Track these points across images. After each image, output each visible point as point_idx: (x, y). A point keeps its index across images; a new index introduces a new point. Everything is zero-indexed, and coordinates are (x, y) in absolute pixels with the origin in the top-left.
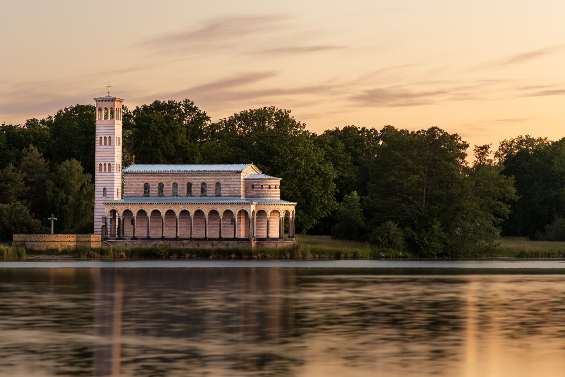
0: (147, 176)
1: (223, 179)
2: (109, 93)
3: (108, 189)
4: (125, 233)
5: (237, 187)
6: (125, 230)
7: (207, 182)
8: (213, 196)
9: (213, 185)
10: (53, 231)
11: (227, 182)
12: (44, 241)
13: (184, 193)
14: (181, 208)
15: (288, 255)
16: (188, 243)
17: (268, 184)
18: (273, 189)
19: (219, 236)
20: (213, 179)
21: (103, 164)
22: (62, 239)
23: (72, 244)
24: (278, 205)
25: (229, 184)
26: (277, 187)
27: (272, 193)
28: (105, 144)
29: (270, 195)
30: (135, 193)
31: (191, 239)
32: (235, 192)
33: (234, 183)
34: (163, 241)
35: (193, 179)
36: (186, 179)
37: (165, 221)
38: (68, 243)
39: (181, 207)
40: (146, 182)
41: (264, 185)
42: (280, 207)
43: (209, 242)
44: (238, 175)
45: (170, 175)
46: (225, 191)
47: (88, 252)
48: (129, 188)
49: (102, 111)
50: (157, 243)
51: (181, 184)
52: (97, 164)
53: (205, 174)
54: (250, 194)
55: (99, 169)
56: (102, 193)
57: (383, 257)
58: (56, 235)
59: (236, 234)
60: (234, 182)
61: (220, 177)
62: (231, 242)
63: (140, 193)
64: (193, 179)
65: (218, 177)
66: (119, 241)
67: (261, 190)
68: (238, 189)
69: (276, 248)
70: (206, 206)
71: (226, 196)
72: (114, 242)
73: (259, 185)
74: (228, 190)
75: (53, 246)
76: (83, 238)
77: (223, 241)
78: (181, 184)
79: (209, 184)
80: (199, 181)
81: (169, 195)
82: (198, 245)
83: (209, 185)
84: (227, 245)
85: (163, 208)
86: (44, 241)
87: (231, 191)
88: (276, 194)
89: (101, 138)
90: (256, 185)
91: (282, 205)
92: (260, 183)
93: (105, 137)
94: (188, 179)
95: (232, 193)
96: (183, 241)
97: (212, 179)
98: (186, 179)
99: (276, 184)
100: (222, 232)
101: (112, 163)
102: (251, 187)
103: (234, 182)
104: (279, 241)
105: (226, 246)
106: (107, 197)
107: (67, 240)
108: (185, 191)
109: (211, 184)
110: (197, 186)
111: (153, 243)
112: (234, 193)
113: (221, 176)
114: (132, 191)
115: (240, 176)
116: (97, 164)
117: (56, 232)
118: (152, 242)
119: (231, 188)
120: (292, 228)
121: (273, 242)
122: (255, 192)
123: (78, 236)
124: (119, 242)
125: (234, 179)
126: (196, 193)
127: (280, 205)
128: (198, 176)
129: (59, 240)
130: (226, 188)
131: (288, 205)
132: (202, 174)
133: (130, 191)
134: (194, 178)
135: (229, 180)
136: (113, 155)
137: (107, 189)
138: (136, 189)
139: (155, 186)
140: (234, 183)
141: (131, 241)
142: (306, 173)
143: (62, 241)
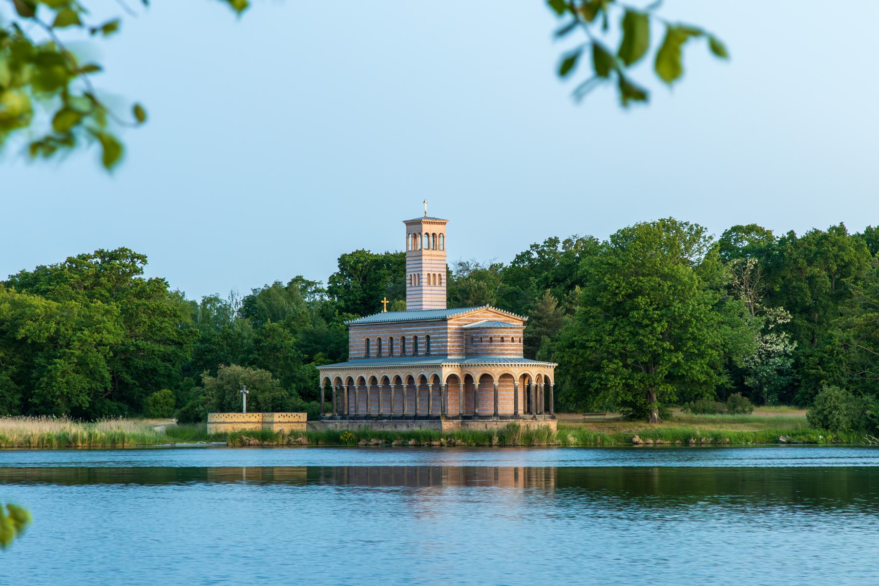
0: (368, 329)
8: (424, 355)
10: (244, 409)
12: (214, 423)
15: (496, 440)
22: (235, 419)
23: (249, 427)
26: (515, 339)
27: (495, 349)
28: (435, 283)
31: (389, 418)
35: (407, 331)
37: (370, 393)
38: (243, 424)
39: (382, 371)
40: (366, 337)
42: (493, 370)
47: (241, 439)
49: (418, 238)
54: (470, 351)
57: (783, 443)
58: (250, 414)
59: (430, 411)
62: (424, 422)
64: (407, 331)
69: (485, 430)
70: (404, 370)
71: (435, 355)
72: (327, 422)
73: (477, 337)
75: (222, 428)
76: (268, 417)
82: (396, 426)
83: (420, 339)
85: (367, 374)
86: (214, 423)
88: (515, 349)
89: (411, 275)
99: (513, 335)
100: (418, 407)
104: (490, 420)
107: (243, 421)
113: (430, 325)
115: (447, 324)
117: (248, 411)
119: (439, 342)
120: (539, 400)
121: (480, 420)
122: (474, 348)
123: (264, 415)
127: (447, 367)
128: (410, 327)
129: (230, 421)
136: (420, 300)
142: (646, 316)
143: (235, 422)
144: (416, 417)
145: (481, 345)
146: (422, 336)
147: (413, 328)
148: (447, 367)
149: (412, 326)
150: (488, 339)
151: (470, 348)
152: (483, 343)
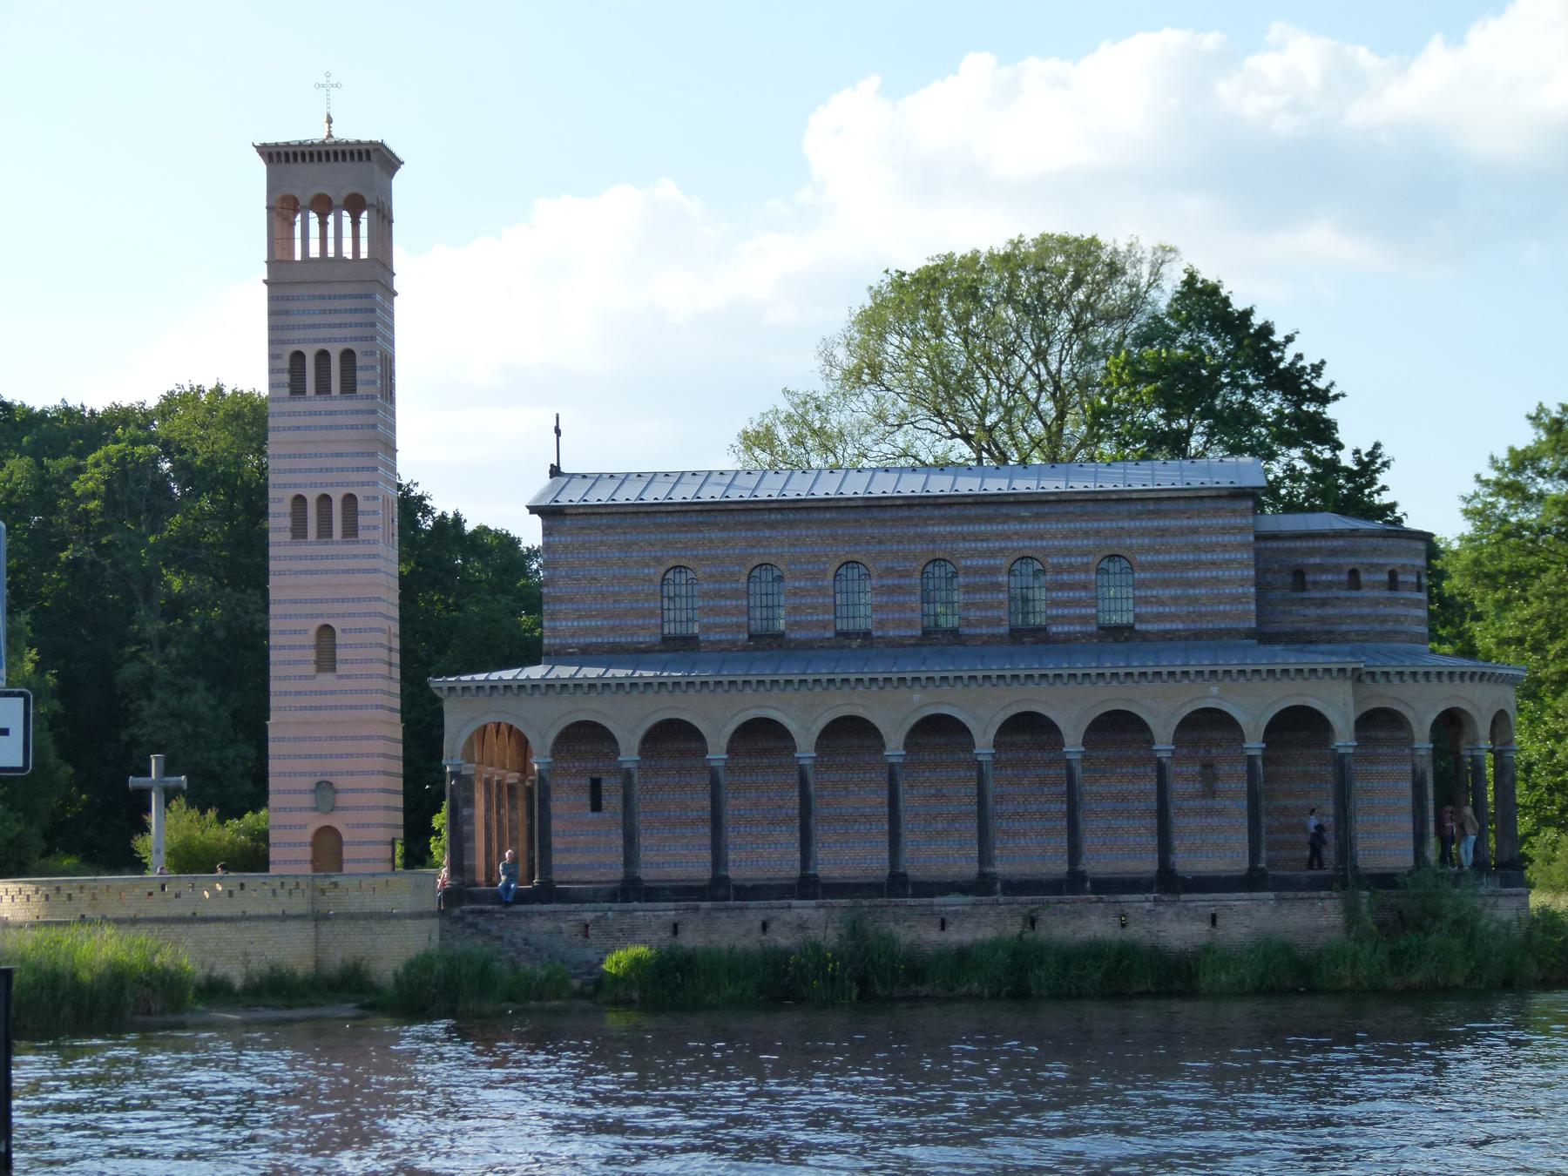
1: (1145, 532)
2: (330, 121)
3: (344, 631)
4: (557, 859)
5: (1227, 582)
6: (557, 843)
7: (1047, 556)
9: (1087, 572)
11: (1167, 552)
13: (910, 624)
14: (922, 703)
16: (967, 909)
17: (1385, 565)
18: (1407, 595)
19: (1065, 868)
20: (1086, 534)
21: (312, 497)
24: (1433, 678)
25: (1185, 565)
29: (1398, 627)
30: (612, 629)
32: (1222, 608)
33: (1209, 556)
34: (812, 903)
36: (920, 536)
41: (1367, 571)
43: (1100, 901)
45: (822, 516)
46: (1161, 603)
48: (572, 601)
50: (775, 913)
51: (890, 571)
52: (281, 500)
53: (1035, 509)
55: (287, 522)
56: (311, 655)
60: (1211, 548)
61: (1126, 524)
63: (642, 627)
65: (1114, 524)
66: (536, 907)
67: (1347, 599)
68: (1240, 590)
73: (1337, 569)
74: (1176, 600)
77: (1183, 897)
78: (890, 571)
79: (1060, 565)
80: (1001, 550)
81: (815, 633)
84: (1214, 919)
87: (1195, 601)
90: (1322, 569)
91: (1445, 678)
92: (1342, 560)
93: (323, 356)
94: (933, 541)
95: (1201, 615)
96: (937, 900)
97: (1075, 533)
98: (920, 536)
101: (368, 490)
102: (1289, 580)
103: (1211, 548)
105: (1206, 926)
106: (341, 677)
108: (913, 610)
109: (1071, 565)
110: (983, 580)
111: (750, 915)
112: (1215, 614)
113: (1132, 516)
114: (591, 617)
116: (281, 500)
118: (790, 907)
122: (1313, 612)
124: (541, 914)
125: (1208, 530)
126: (981, 622)
128: (990, 520)
130: (1166, 584)
131: (1489, 680)
132: (1014, 510)
133: (580, 617)
134: (972, 533)
135: (1183, 540)
137: (338, 631)
138: (615, 601)
139: (728, 586)
140: (1209, 556)
141: (616, 906)
144: (1168, 882)
145: (1356, 599)
148: (1433, 678)
149: (1006, 519)
150: (1385, 577)
151: (1283, 613)
152: (1367, 593)
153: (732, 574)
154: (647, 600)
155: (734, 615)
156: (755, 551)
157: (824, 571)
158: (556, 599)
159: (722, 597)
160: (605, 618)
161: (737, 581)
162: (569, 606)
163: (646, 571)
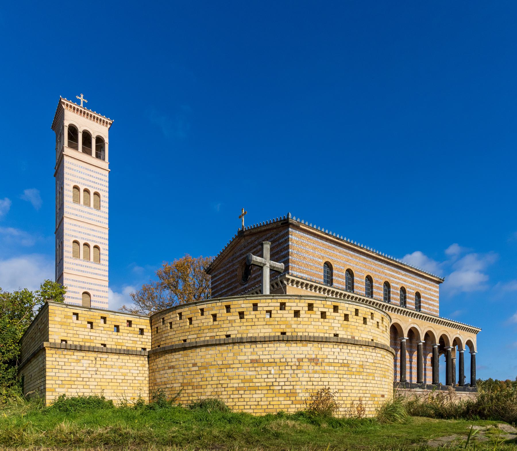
44: (436, 286)
48: (298, 264)
94: (386, 275)
128: (397, 272)
133: (300, 272)
146: (412, 291)
147: (400, 276)
153: (342, 269)
154: (320, 272)
155: (342, 285)
156: (347, 263)
157: (363, 276)
158: (294, 262)
159: (339, 277)
160: (308, 275)
161: (343, 272)
162: (297, 266)
163: (319, 260)
